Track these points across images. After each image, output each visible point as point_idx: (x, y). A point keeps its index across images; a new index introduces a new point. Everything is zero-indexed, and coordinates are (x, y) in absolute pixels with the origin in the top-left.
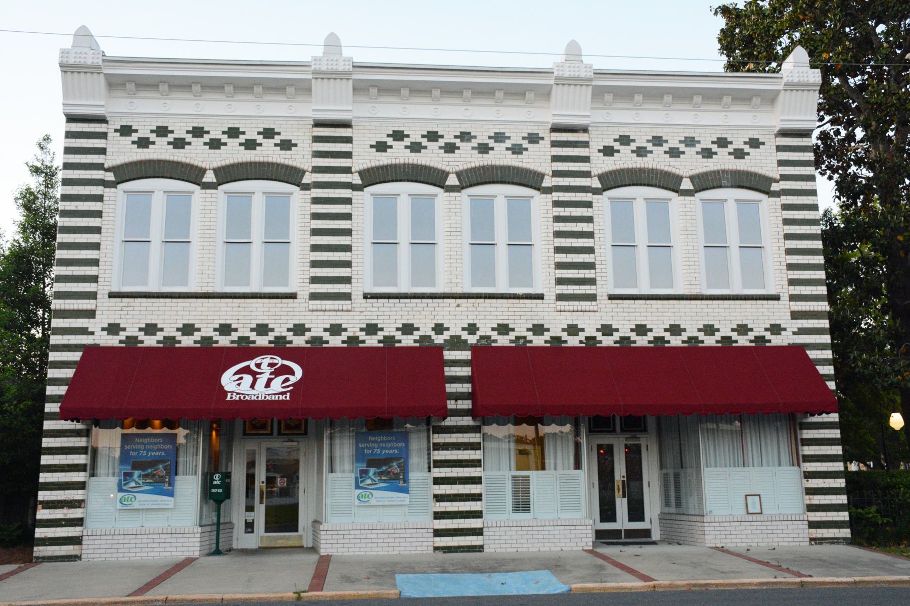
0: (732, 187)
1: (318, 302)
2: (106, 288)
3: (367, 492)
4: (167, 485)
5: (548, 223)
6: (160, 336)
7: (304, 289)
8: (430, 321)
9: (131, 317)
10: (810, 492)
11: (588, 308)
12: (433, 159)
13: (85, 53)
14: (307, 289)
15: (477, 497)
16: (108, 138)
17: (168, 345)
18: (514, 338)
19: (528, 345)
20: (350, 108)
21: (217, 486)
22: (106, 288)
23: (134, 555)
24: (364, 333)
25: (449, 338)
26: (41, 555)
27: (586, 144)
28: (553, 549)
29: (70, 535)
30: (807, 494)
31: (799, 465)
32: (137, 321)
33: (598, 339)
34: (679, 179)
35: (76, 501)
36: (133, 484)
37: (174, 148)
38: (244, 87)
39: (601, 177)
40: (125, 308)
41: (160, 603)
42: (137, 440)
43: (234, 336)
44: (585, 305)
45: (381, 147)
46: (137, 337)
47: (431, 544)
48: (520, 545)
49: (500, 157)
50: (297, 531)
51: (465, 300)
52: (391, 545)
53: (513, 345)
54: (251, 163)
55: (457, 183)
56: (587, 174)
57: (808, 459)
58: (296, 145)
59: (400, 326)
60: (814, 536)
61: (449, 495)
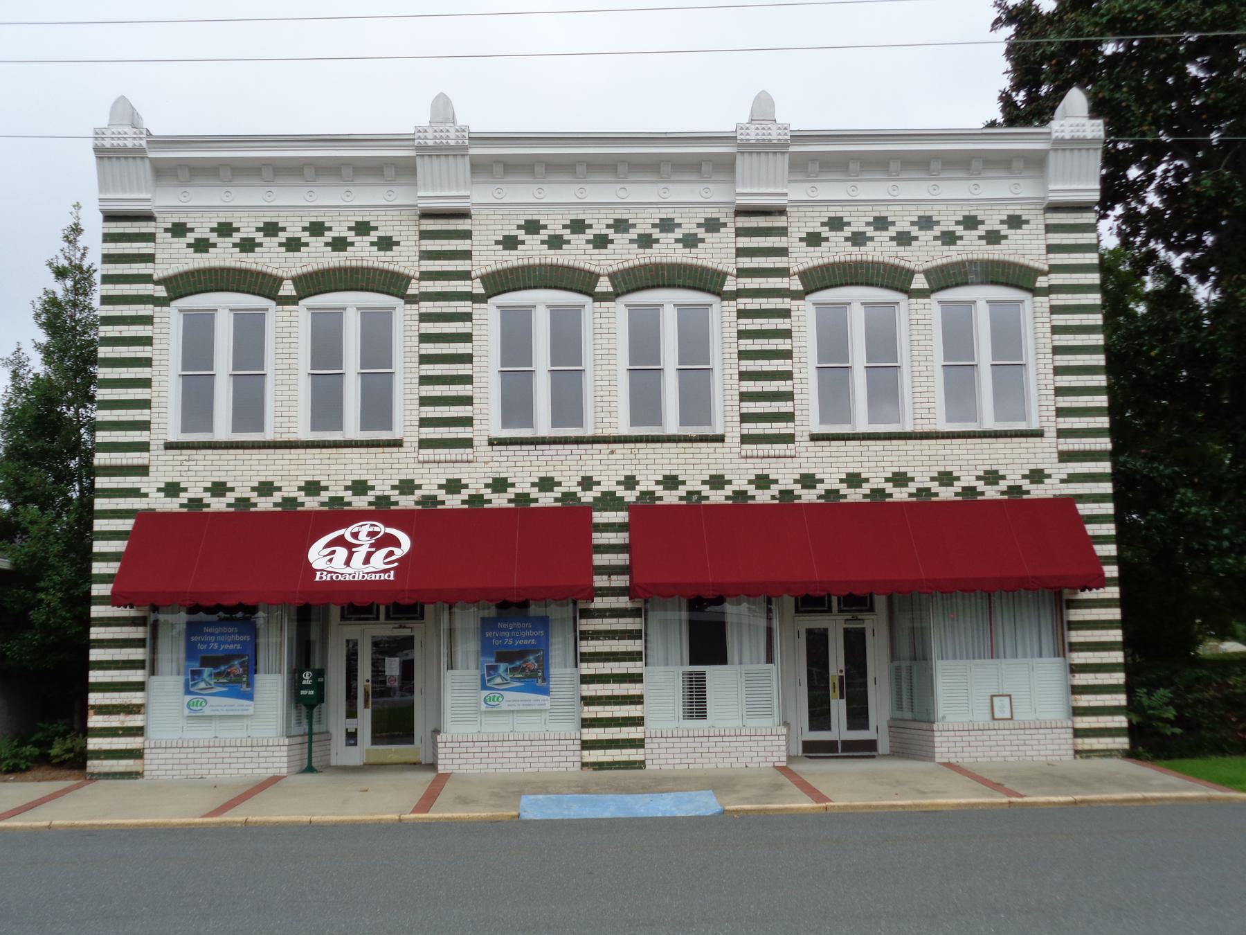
1: (430, 451)
2: (161, 436)
6: (230, 498)
11: (782, 453)
12: (578, 257)
16: (157, 241)
19: (703, 502)
21: (307, 687)
22: (161, 436)
24: (489, 490)
25: (599, 495)
26: (97, 770)
27: (782, 231)
29: (129, 747)
33: (796, 493)
34: (910, 274)
39: (803, 275)
40: (185, 463)
42: (206, 630)
44: (779, 448)
45: (510, 243)
49: (668, 251)
51: (621, 445)
54: (340, 269)
58: (398, 244)
59: (537, 480)
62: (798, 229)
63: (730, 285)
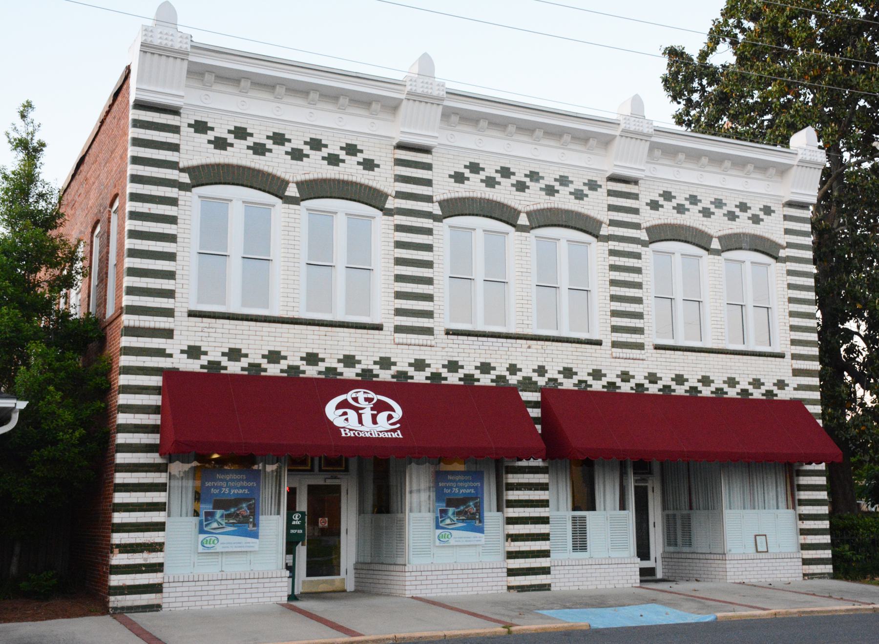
0: (750, 250)
1: (404, 335)
2: (184, 305)
3: (447, 532)
4: (251, 526)
5: (604, 271)
6: (244, 362)
7: (391, 321)
8: (505, 361)
9: (212, 339)
10: (804, 532)
11: (638, 357)
12: (506, 196)
13: (172, 35)
14: (392, 321)
15: (545, 537)
16: (181, 133)
17: (253, 373)
18: (577, 382)
19: (589, 389)
20: (436, 135)
21: (296, 527)
22: (184, 305)
23: (219, 602)
24: (446, 370)
25: (521, 379)
26: (120, 605)
27: (635, 197)
28: (609, 586)
29: (151, 582)
30: (801, 534)
31: (794, 508)
32: (220, 345)
35: (157, 544)
36: (215, 525)
37: (254, 153)
38: (331, 96)
39: (649, 230)
40: (206, 330)
41: (391, 642)
43: (322, 366)
44: (635, 353)
45: (459, 178)
46: (229, 360)
47: (505, 583)
48: (581, 584)
49: (564, 200)
50: (339, 574)
51: (535, 342)
52: (470, 585)
53: (576, 388)
54: (334, 180)
55: (528, 223)
56: (637, 226)
57: (802, 503)
58: (378, 166)
59: (479, 365)
60: (807, 572)
61: (522, 535)
62: (646, 197)
63: (391, 204)
